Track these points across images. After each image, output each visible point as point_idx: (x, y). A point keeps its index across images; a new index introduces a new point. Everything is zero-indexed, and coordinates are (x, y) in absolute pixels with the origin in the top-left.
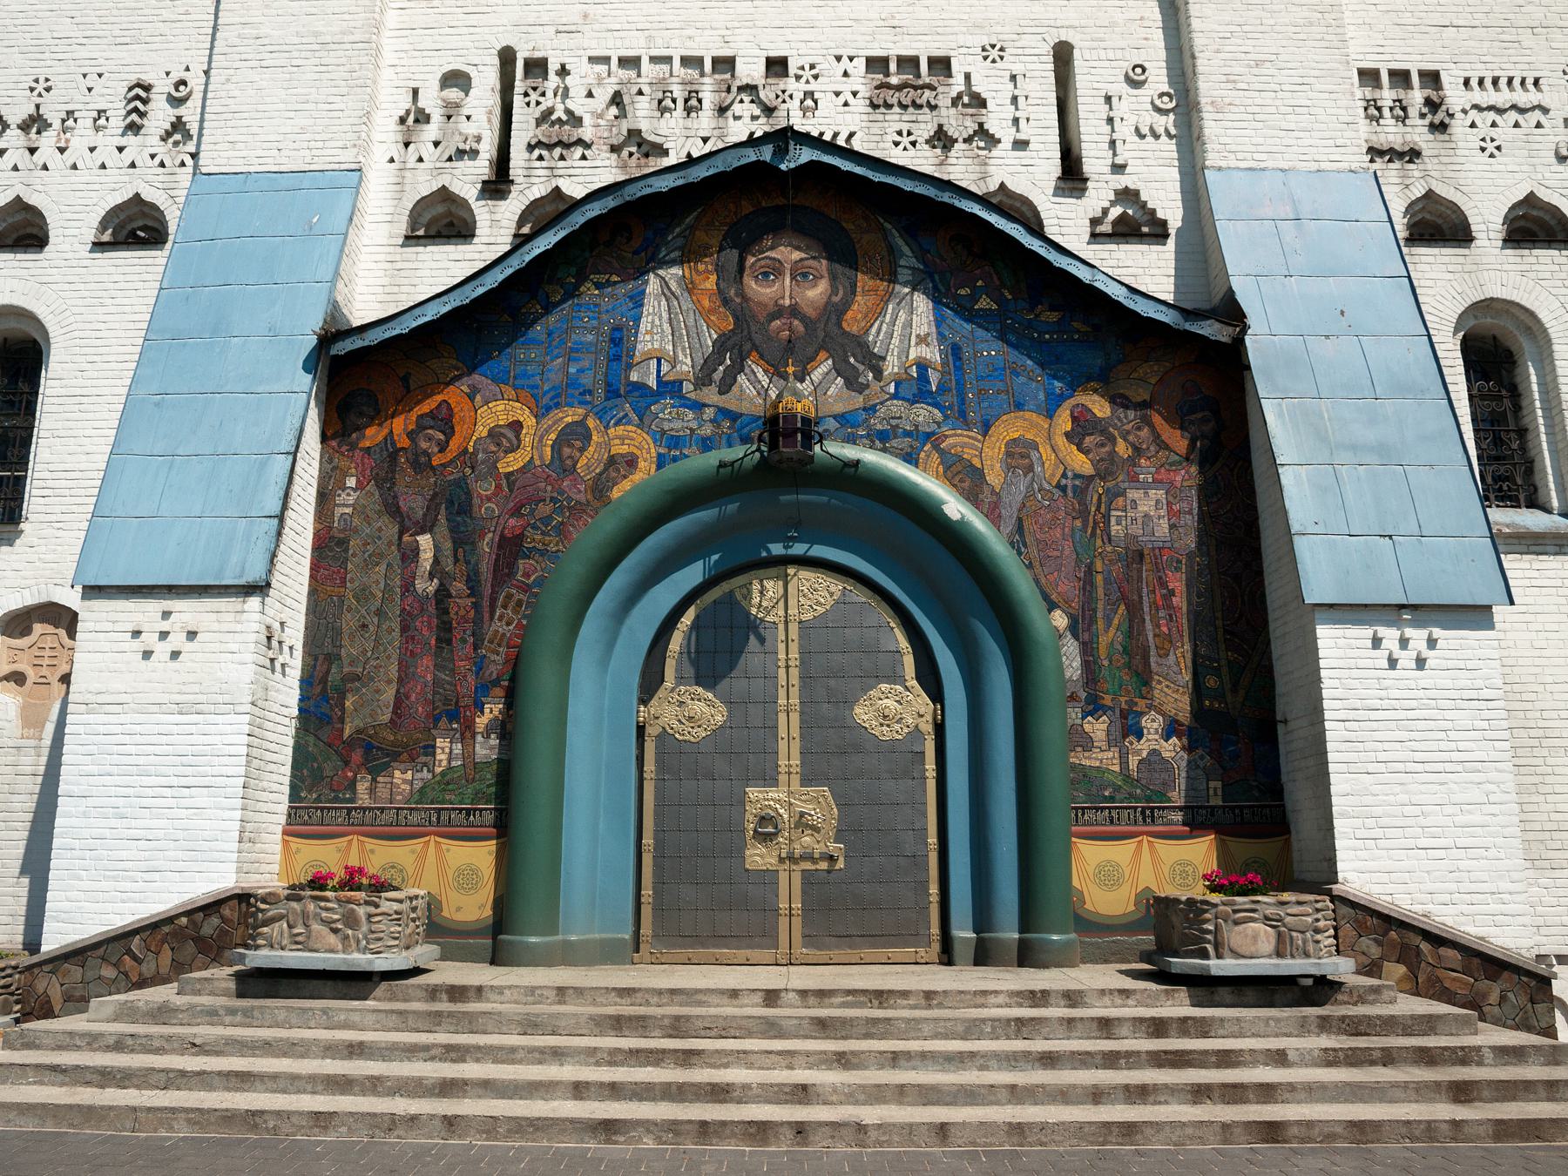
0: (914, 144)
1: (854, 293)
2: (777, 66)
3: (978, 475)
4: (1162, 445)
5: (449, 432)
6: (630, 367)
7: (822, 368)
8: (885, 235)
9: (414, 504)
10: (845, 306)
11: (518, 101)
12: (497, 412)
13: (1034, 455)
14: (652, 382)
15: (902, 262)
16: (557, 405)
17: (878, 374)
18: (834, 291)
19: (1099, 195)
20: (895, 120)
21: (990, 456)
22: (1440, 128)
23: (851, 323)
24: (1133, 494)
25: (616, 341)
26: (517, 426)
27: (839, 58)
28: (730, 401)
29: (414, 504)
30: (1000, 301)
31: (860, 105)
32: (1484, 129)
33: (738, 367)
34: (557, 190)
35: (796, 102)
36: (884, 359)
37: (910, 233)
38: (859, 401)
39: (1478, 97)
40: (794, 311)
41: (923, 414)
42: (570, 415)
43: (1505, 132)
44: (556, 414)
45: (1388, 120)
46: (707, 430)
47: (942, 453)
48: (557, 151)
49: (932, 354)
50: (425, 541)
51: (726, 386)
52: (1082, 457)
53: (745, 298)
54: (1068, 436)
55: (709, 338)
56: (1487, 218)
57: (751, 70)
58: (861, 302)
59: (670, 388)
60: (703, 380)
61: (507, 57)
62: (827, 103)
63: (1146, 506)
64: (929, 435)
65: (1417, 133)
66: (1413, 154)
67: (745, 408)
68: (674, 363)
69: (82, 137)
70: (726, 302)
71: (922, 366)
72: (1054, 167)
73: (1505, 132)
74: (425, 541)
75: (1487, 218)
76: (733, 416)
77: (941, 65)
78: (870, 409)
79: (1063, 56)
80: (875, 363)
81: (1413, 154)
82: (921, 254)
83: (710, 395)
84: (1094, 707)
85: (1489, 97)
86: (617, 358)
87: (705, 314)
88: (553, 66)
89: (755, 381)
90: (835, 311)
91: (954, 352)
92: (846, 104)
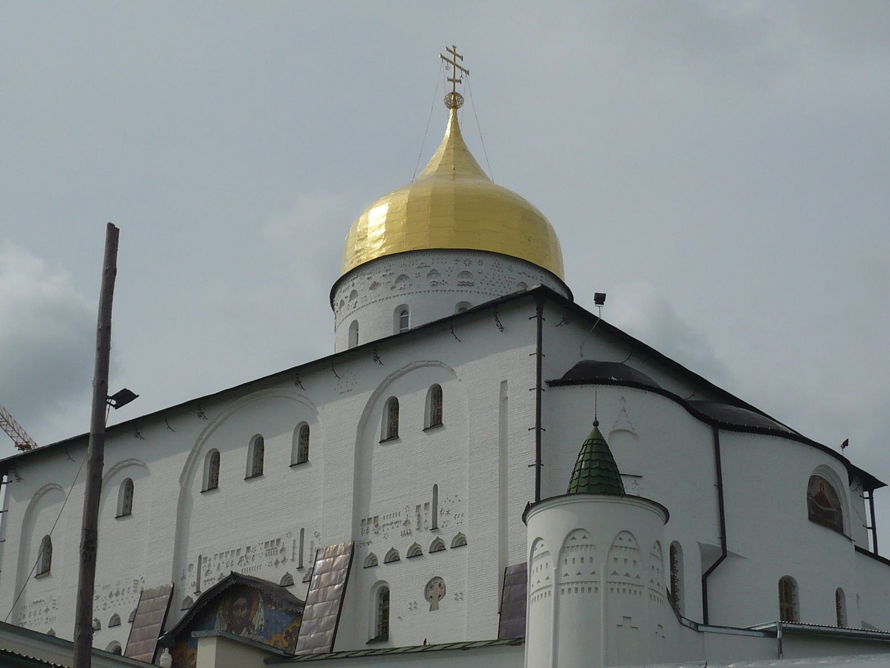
0: (272, 565)
2: (248, 548)
11: (202, 569)
13: (278, 644)
15: (260, 601)
27: (260, 544)
35: (251, 558)
36: (255, 626)
49: (264, 623)
52: (286, 642)
54: (285, 638)
61: (200, 557)
77: (278, 540)
85: (389, 522)
90: (248, 615)
91: (267, 621)
92: (260, 557)
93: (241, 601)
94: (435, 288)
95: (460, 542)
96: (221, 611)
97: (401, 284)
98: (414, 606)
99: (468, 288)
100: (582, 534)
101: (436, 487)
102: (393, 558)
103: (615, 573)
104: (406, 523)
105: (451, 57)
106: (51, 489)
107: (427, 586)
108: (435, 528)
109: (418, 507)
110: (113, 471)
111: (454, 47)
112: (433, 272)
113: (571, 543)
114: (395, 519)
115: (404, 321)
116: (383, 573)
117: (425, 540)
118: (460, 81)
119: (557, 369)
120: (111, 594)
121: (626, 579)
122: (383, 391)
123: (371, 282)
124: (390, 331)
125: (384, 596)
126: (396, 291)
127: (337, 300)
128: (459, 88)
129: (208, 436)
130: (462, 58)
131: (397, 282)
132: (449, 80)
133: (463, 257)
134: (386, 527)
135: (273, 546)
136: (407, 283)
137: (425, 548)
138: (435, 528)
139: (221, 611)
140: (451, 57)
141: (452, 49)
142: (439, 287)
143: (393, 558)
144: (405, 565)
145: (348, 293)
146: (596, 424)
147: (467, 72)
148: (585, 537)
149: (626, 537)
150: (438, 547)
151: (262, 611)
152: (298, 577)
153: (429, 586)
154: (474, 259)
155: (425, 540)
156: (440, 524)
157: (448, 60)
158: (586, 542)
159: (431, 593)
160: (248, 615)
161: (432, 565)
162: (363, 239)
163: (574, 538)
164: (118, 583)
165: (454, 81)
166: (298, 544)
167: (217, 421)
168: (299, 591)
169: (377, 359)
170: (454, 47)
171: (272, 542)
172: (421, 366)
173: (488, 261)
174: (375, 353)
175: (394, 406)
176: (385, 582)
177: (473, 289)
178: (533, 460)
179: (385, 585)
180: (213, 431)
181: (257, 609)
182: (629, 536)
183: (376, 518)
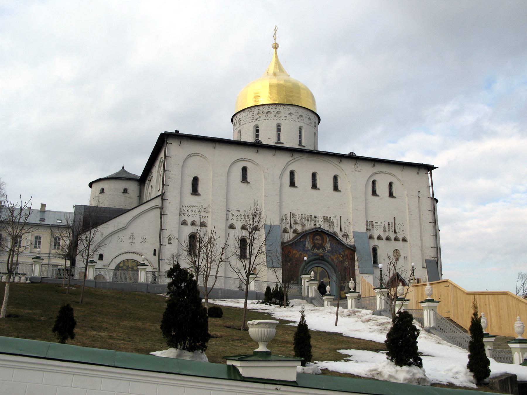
1: (323, 242)
3: (333, 260)
4: (348, 258)
5: (290, 253)
6: (305, 248)
8: (326, 237)
9: (288, 260)
10: (323, 243)
12: (295, 252)
14: (307, 250)
16: (300, 251)
17: (326, 250)
18: (322, 242)
19: (343, 233)
20: (326, 223)
22: (373, 227)
23: (323, 245)
24: (346, 262)
25: (304, 246)
26: (296, 253)
28: (313, 252)
29: (288, 260)
30: (335, 244)
31: (323, 222)
32: (376, 227)
33: (314, 249)
34: (296, 228)
37: (328, 237)
38: (324, 253)
40: (319, 244)
41: (329, 254)
42: (300, 252)
43: (378, 228)
44: (299, 252)
45: (368, 226)
46: (312, 254)
47: (331, 258)
48: (296, 224)
49: (330, 249)
50: (289, 263)
51: (313, 250)
53: (315, 242)
55: (312, 246)
56: (376, 237)
57: (313, 217)
58: (324, 243)
59: (309, 250)
60: (311, 250)
61: (291, 213)
62: (320, 221)
63: (346, 263)
64: (330, 256)
65: (371, 228)
66: (370, 230)
67: (314, 253)
68: (309, 248)
70: (313, 242)
71: (329, 249)
73: (378, 228)
74: (289, 263)
76: (314, 253)
78: (325, 253)
79: (341, 217)
80: (325, 249)
81: (370, 230)
82: (329, 238)
83: (312, 251)
84: (342, 280)
86: (304, 247)
87: (311, 244)
88: (295, 215)
89: (315, 250)
90: (322, 244)
91: (332, 248)
93: (318, 237)
95: (404, 240)
96: (308, 239)
97: (300, 118)
101: (394, 218)
102: (379, 238)
106: (197, 155)
108: (395, 232)
110: (238, 160)
112: (309, 119)
114: (380, 225)
116: (376, 242)
117: (392, 236)
123: (289, 112)
126: (299, 120)
134: (376, 227)
137: (393, 238)
138: (395, 232)
143: (379, 238)
150: (396, 239)
151: (329, 244)
160: (322, 244)
164: (245, 211)
167: (295, 160)
174: (374, 163)
181: (326, 242)
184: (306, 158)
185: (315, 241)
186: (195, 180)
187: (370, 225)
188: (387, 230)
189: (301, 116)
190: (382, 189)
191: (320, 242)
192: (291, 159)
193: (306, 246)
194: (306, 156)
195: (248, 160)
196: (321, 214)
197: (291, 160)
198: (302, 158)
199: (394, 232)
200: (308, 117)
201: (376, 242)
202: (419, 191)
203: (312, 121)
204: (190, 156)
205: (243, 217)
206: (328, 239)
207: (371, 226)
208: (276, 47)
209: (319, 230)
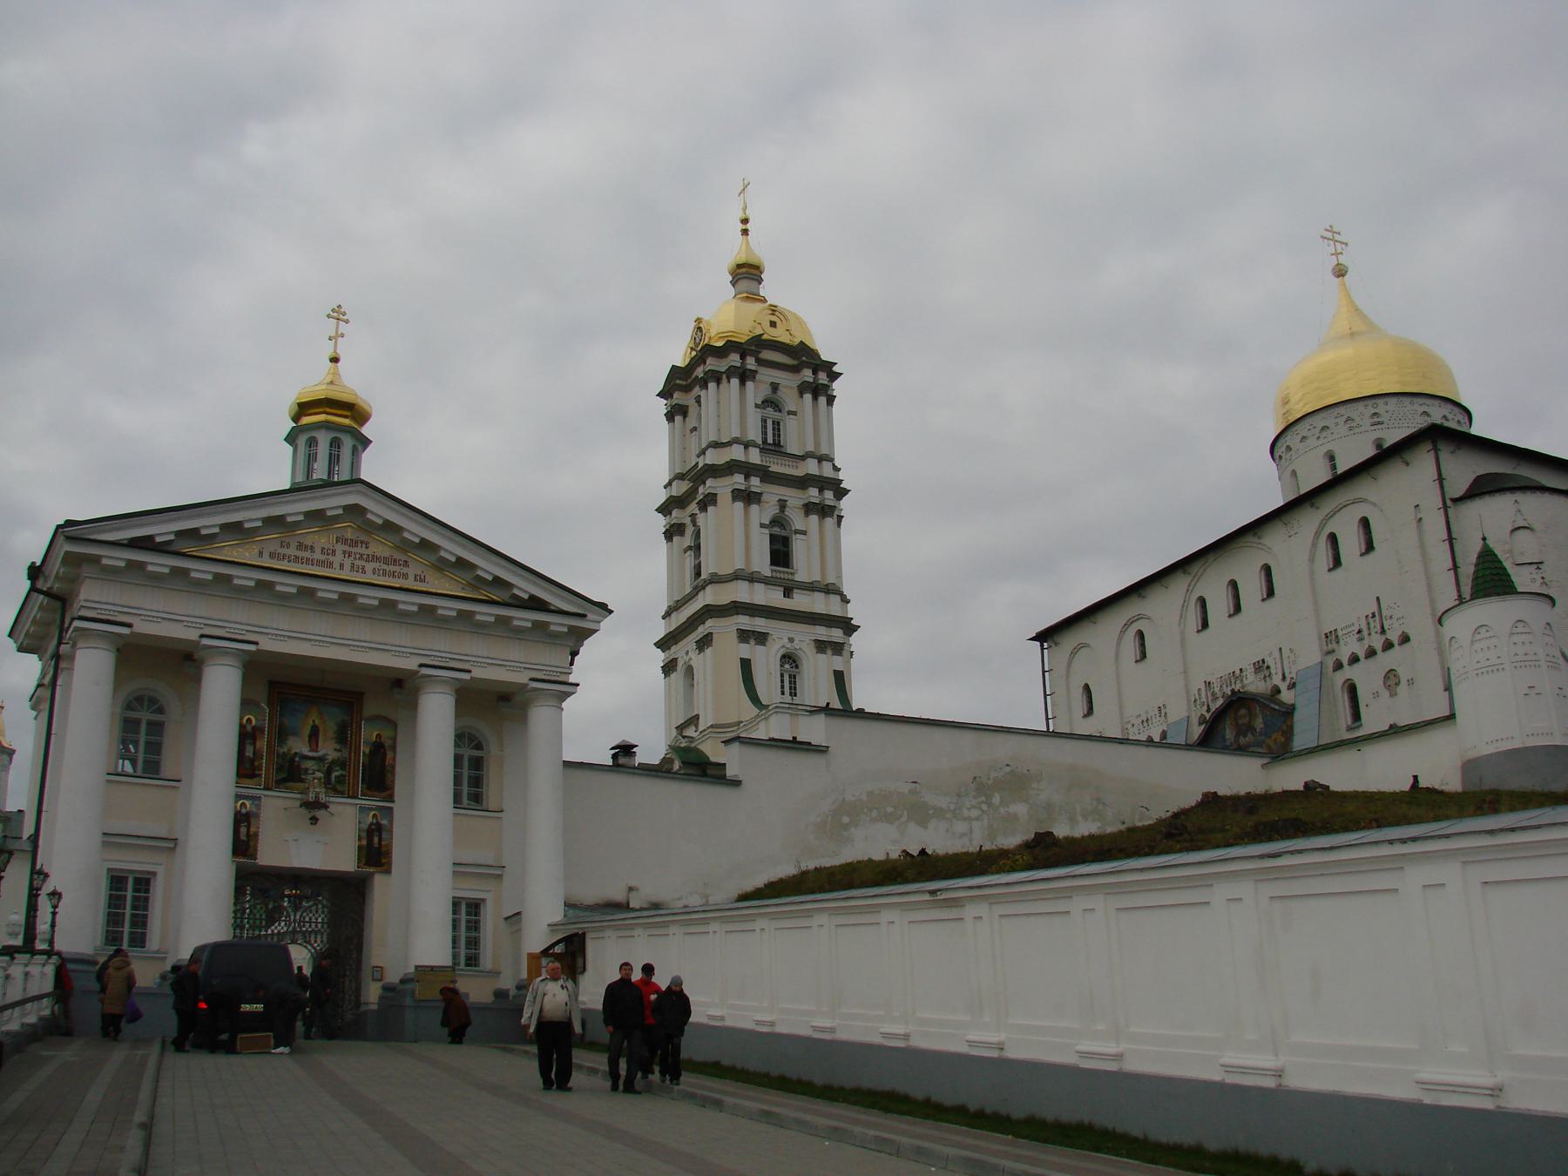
2: (1241, 670)
7: (1249, 735)
19: (1288, 680)
20: (1259, 676)
21: (1271, 743)
22: (1338, 642)
39: (1344, 632)
41: (1263, 737)
56: (1345, 662)
57: (1238, 672)
62: (1248, 676)
65: (1334, 646)
66: (1333, 651)
69: (1154, 721)
72: (1281, 677)
75: (1345, 662)
80: (1255, 730)
81: (1333, 651)
90: (1250, 722)
93: (1243, 712)
94: (1352, 432)
95: (1405, 639)
97: (1324, 434)
98: (1376, 695)
99: (1379, 426)
100: (1484, 629)
101: (1378, 598)
102: (1354, 659)
103: (1516, 654)
104: (1359, 632)
105: (1329, 235)
107: (1385, 677)
109: (1367, 616)
111: (1331, 227)
112: (1349, 419)
113: (1478, 637)
114: (1349, 630)
115: (1334, 467)
117: (1377, 642)
118: (1341, 253)
119: (1459, 485)
120: (1143, 721)
121: (1525, 658)
122: (1322, 529)
124: (1323, 476)
125: (1352, 690)
127: (1276, 455)
128: (1342, 260)
129: (1193, 588)
130: (1339, 234)
131: (1320, 432)
132: (1333, 254)
133: (1370, 402)
135: (1260, 666)
136: (1329, 431)
137: (1378, 646)
138: (1383, 631)
139: (1228, 722)
140: (1329, 235)
141: (1329, 228)
142: (1356, 430)
143: (1354, 659)
144: (1363, 663)
145: (1283, 449)
146: (1484, 539)
147: (1346, 244)
148: (1487, 631)
149: (1519, 624)
150: (1388, 645)
151: (1260, 717)
152: (1283, 686)
153: (1386, 677)
154: (1380, 402)
155: (1377, 642)
156: (1386, 627)
157: (1328, 239)
158: (1488, 635)
159: (1389, 683)
160: (1250, 722)
161: (1385, 661)
162: (1287, 402)
163: (1479, 633)
164: (1147, 712)
165: (1336, 254)
166: (1278, 661)
167: (1199, 574)
168: (1286, 696)
169: (1312, 506)
170: (1331, 227)
171: (1258, 662)
172: (1348, 505)
173: (1393, 400)
175: (1333, 538)
176: (1349, 679)
177: (1383, 426)
178: (1450, 564)
179: (1350, 682)
180: (1196, 582)
182: (1522, 624)
183: (1336, 630)
184: (1215, 560)
185: (1240, 722)
186: (1087, 688)
187: (1331, 637)
188: (1365, 633)
189: (1324, 428)
190: (1350, 543)
191: (1247, 719)
192: (1190, 579)
193: (1227, 737)
194: (1211, 557)
195: (1139, 617)
196: (1243, 659)
197: (1192, 580)
198: (1207, 564)
199: (1379, 632)
200: (1341, 420)
201: (1349, 672)
202: (1418, 506)
203: (1358, 420)
204: (1074, 653)
205: (1145, 724)
206: (1258, 708)
207: (1334, 643)
208: (1340, 272)
209: (1234, 699)
